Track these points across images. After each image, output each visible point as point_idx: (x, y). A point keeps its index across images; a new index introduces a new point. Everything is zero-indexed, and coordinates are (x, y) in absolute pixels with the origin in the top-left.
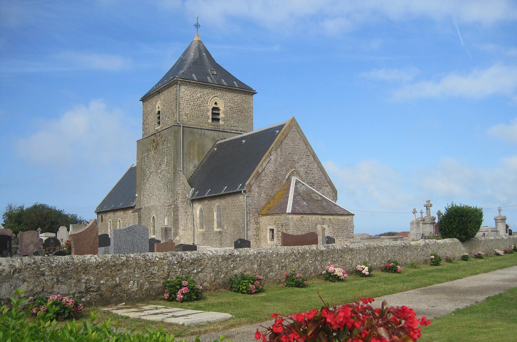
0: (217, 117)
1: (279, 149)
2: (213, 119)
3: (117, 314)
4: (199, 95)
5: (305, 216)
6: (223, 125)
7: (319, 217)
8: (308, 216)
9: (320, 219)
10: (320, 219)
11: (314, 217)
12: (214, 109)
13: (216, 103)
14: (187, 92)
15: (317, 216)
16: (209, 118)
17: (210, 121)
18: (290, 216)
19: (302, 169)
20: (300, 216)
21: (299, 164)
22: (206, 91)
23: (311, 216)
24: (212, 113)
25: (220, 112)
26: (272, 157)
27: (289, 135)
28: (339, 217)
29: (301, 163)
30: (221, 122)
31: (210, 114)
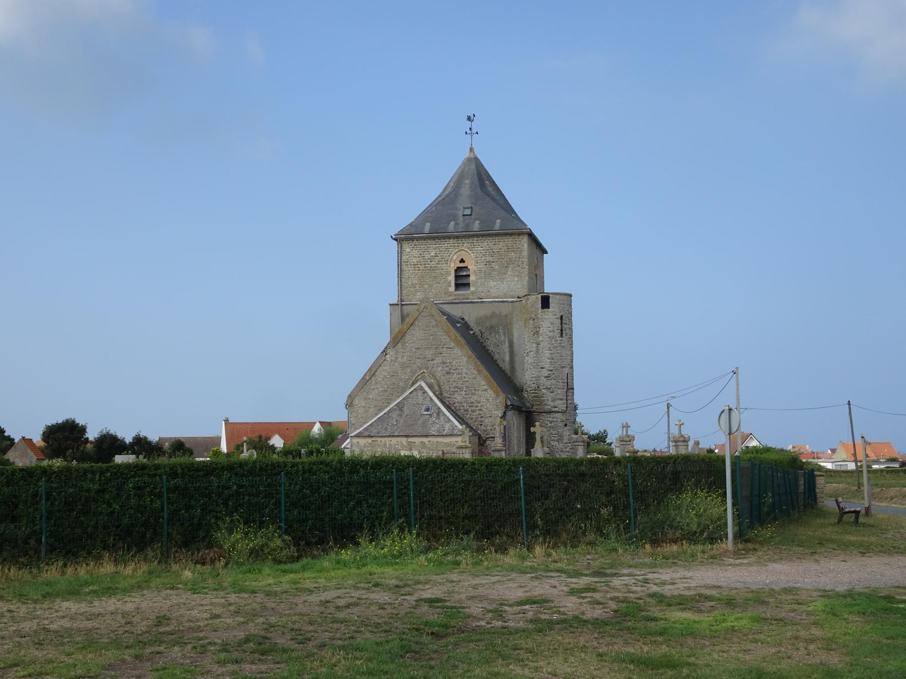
0: (464, 281)
1: (399, 345)
2: (458, 286)
3: (898, 608)
4: (433, 254)
5: (379, 439)
6: (473, 293)
7: (404, 440)
8: (383, 440)
9: (404, 443)
10: (404, 443)
11: (394, 441)
12: (458, 269)
13: (462, 261)
14: (415, 252)
15: (399, 439)
16: (450, 286)
17: (452, 288)
18: (355, 440)
19: (440, 369)
20: (370, 440)
21: (435, 362)
22: (444, 245)
23: (390, 439)
24: (457, 277)
25: (471, 273)
26: (388, 356)
27: (416, 323)
28: (440, 439)
29: (438, 360)
30: (472, 289)
31: (452, 278)
